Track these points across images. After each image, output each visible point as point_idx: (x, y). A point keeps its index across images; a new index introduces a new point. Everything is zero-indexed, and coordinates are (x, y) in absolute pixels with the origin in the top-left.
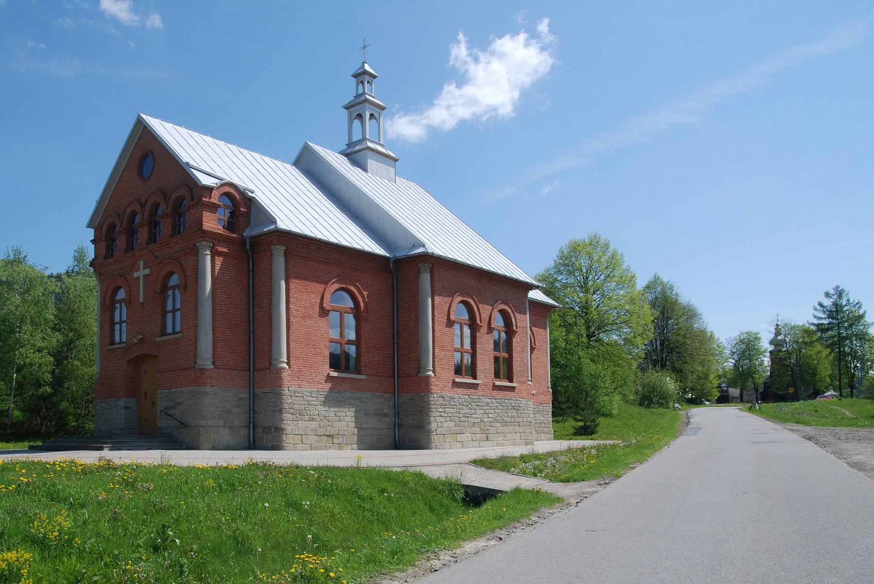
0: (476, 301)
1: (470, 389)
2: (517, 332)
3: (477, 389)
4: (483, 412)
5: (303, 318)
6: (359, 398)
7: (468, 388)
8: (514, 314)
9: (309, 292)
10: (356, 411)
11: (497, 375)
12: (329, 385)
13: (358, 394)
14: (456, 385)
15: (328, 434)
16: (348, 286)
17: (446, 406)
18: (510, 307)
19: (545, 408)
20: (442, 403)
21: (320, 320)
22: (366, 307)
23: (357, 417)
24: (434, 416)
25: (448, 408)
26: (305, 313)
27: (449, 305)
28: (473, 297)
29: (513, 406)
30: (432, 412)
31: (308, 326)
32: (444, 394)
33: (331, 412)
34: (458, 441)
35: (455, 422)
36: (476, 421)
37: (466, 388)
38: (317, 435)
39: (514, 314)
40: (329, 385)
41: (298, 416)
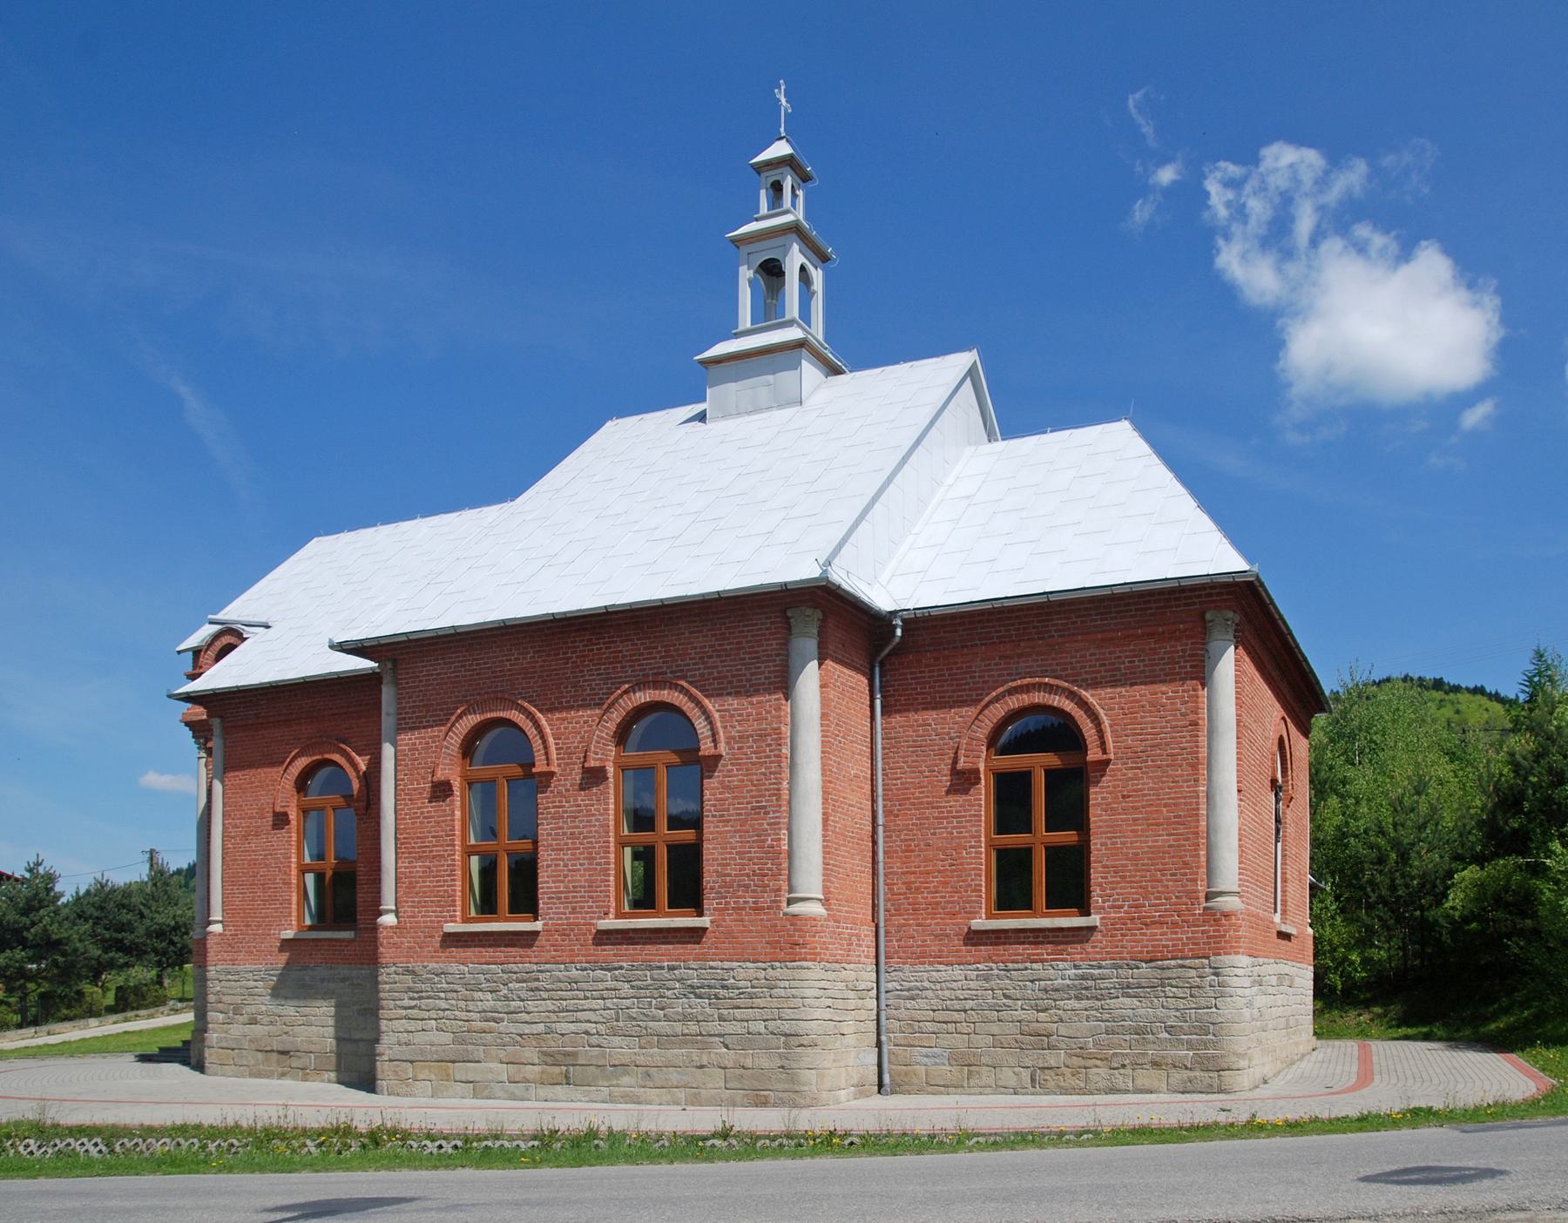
0: (1034, 685)
1: (506, 946)
2: (718, 757)
3: (531, 946)
4: (552, 1008)
5: (246, 837)
6: (347, 979)
7: (500, 946)
8: (699, 704)
9: (257, 787)
10: (337, 1006)
11: (488, 906)
12: (285, 957)
13: (345, 971)
14: (457, 941)
15: (280, 1049)
16: (327, 756)
17: (424, 994)
18: (682, 690)
19: (1168, 973)
20: (409, 988)
21: (275, 834)
22: (364, 783)
23: (339, 1018)
24: (386, 1016)
25: (428, 998)
26: (249, 827)
27: (986, 712)
28: (677, 685)
29: (691, 986)
30: (383, 1009)
31: (253, 851)
32: (416, 966)
33: (289, 1010)
34: (457, 1079)
35: (453, 1033)
36: (527, 1031)
37: (490, 946)
38: (261, 1051)
39: (699, 704)
40: (285, 957)
41: (231, 1014)
